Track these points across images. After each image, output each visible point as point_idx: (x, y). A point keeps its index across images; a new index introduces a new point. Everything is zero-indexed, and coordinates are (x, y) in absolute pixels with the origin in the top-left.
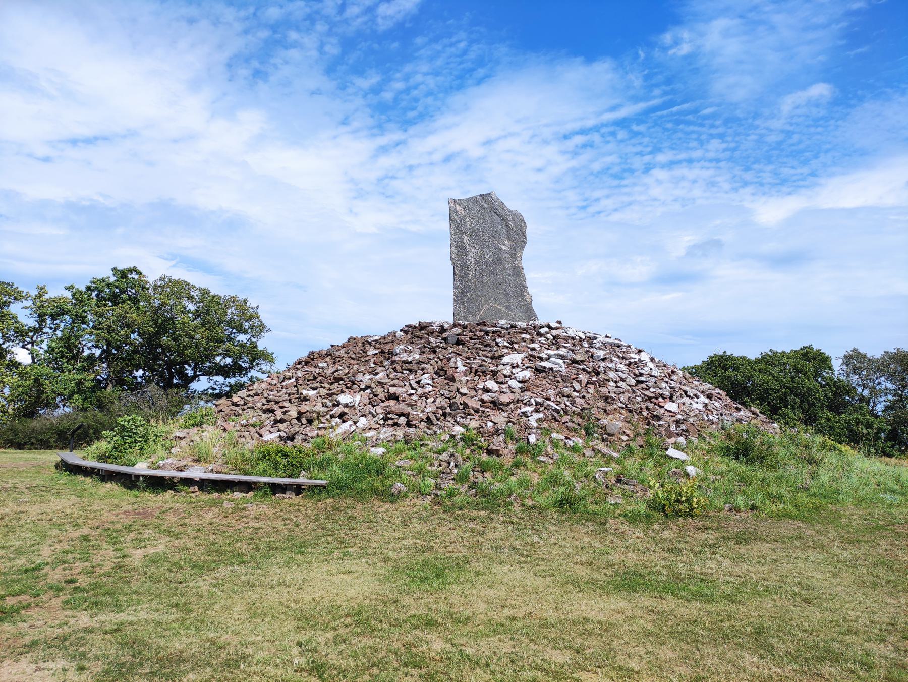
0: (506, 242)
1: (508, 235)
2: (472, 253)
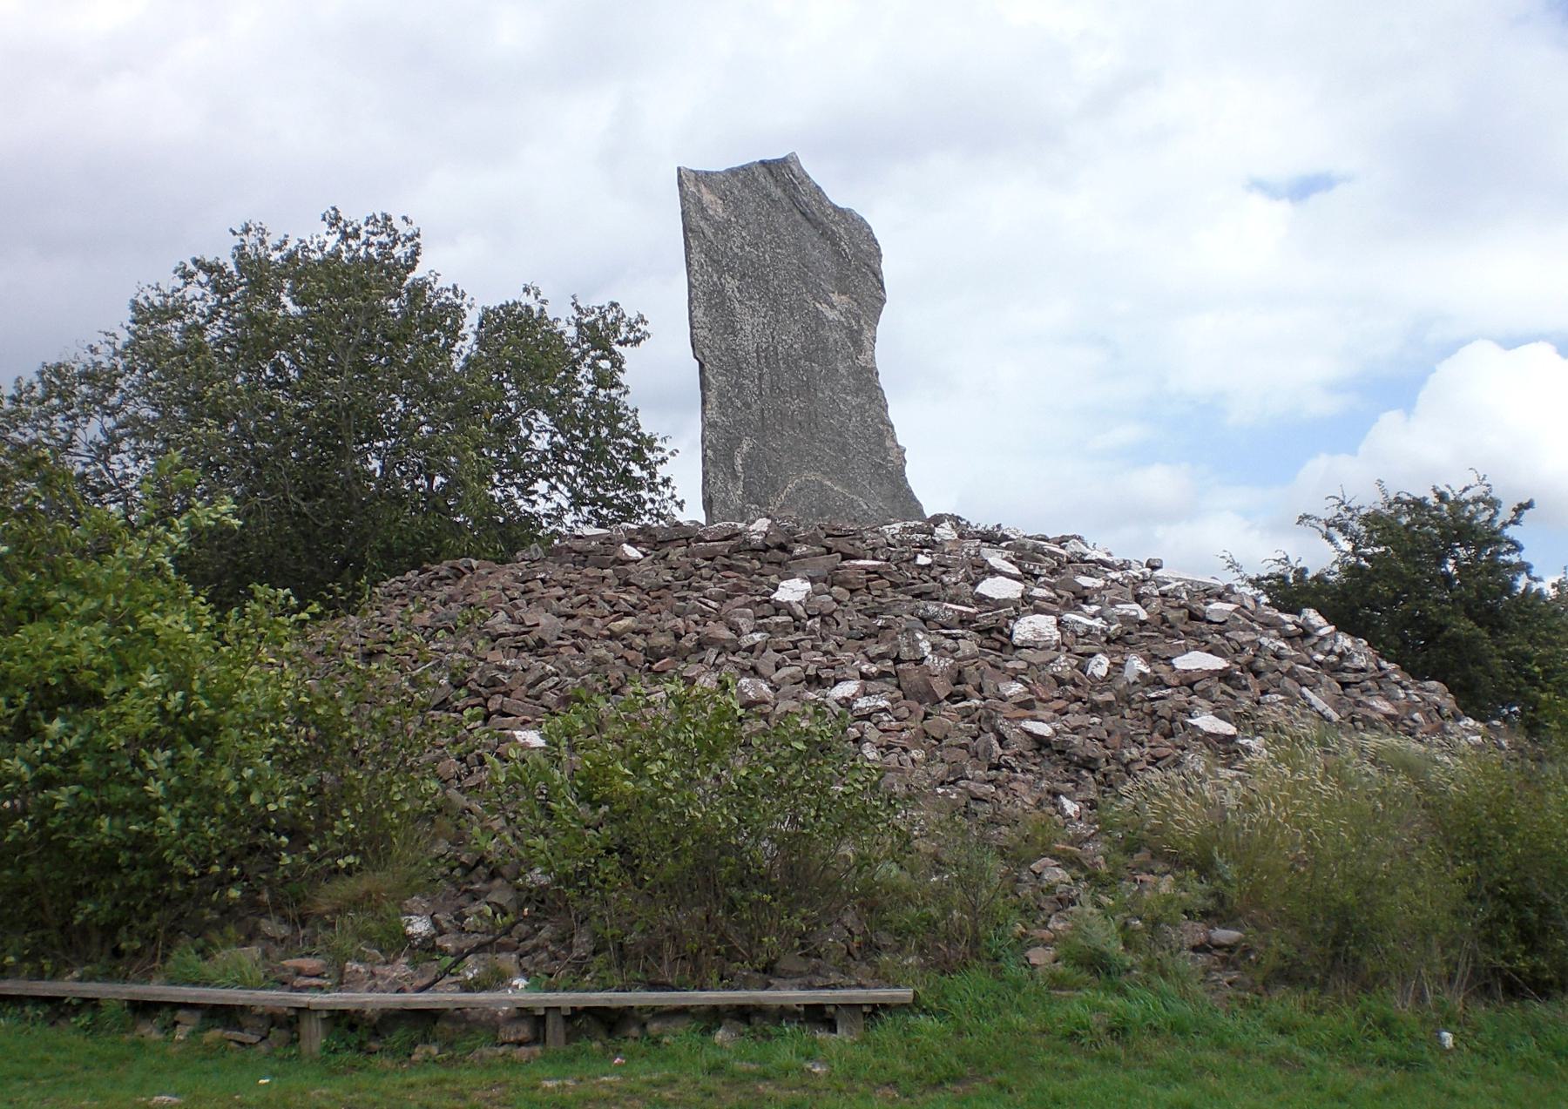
0: (835, 297)
1: (839, 280)
2: (752, 326)
